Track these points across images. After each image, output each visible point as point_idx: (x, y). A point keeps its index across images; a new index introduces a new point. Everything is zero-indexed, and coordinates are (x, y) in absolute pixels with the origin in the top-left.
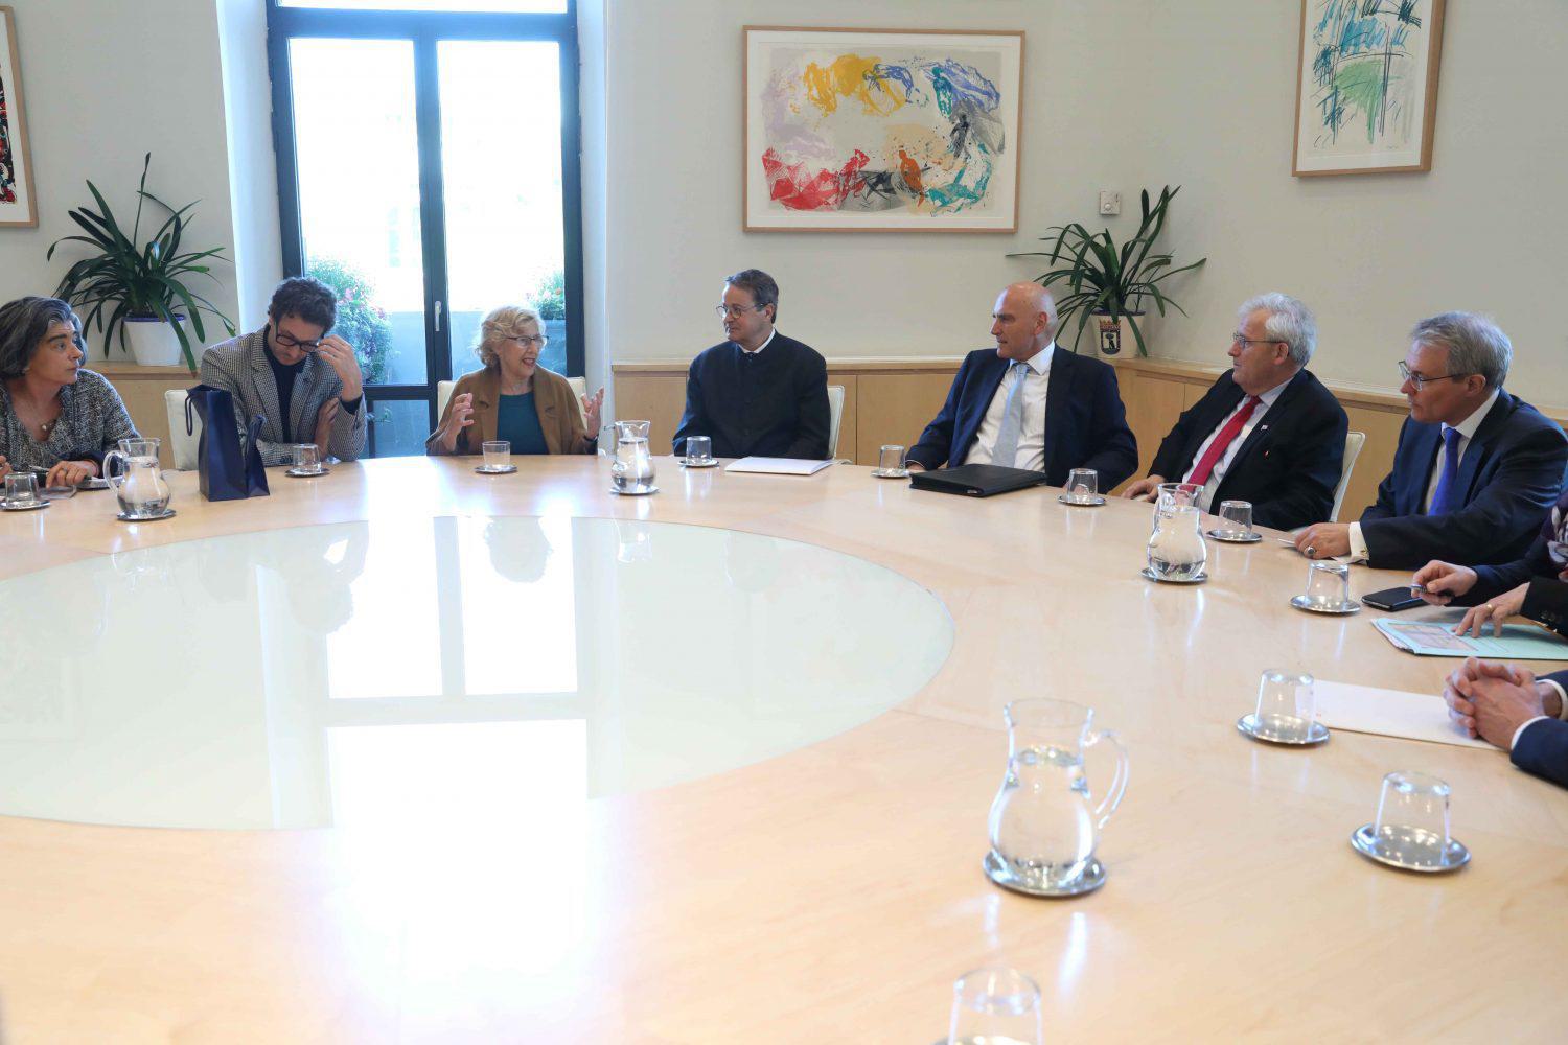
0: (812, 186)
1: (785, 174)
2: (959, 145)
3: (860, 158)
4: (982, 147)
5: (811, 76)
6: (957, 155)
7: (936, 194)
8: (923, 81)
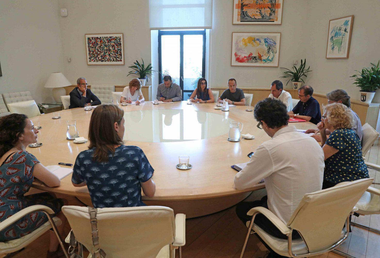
0: (243, 59)
1: (238, 57)
4: (273, 52)
6: (268, 54)
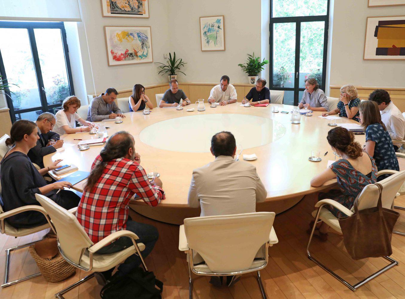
0: (120, 56)
1: (115, 54)
2: (143, 47)
3: (127, 51)
4: (146, 47)
5: (117, 35)
6: (143, 49)
7: (140, 56)
8: (136, 36)
